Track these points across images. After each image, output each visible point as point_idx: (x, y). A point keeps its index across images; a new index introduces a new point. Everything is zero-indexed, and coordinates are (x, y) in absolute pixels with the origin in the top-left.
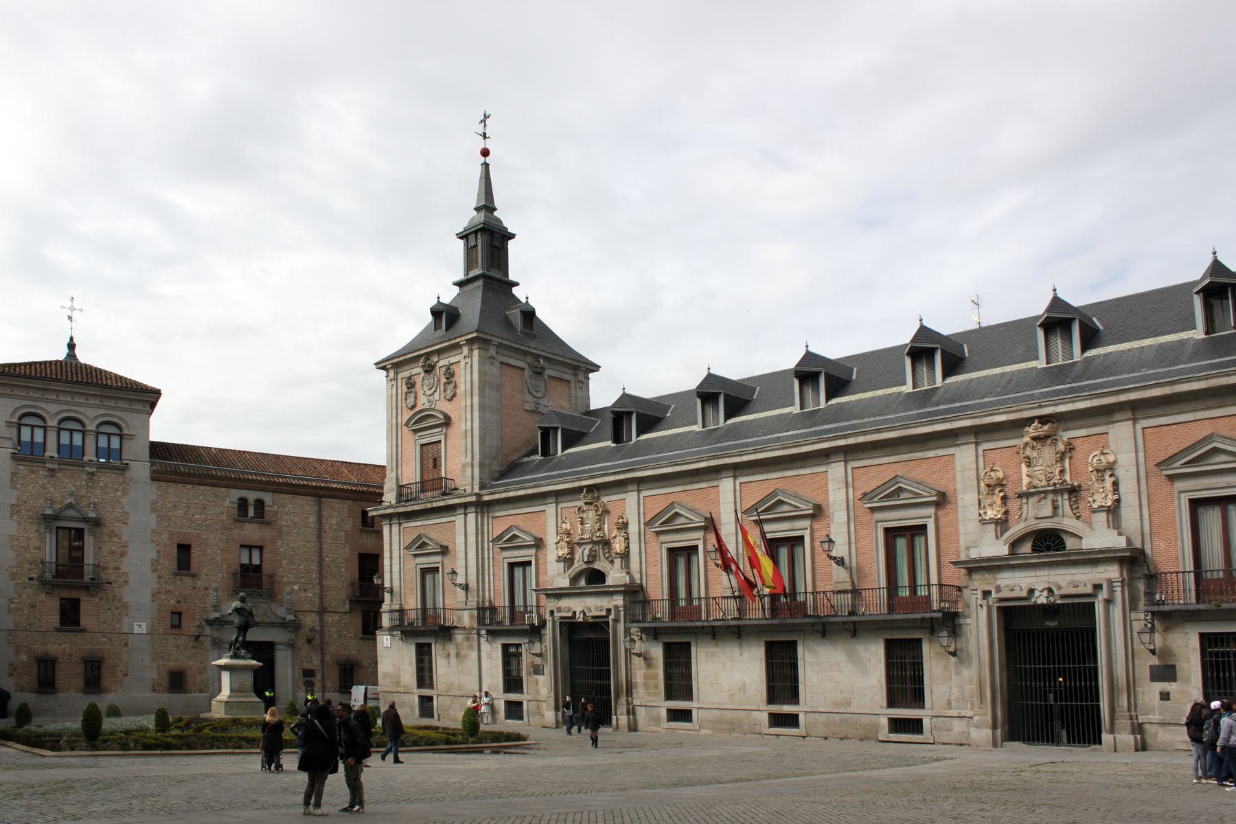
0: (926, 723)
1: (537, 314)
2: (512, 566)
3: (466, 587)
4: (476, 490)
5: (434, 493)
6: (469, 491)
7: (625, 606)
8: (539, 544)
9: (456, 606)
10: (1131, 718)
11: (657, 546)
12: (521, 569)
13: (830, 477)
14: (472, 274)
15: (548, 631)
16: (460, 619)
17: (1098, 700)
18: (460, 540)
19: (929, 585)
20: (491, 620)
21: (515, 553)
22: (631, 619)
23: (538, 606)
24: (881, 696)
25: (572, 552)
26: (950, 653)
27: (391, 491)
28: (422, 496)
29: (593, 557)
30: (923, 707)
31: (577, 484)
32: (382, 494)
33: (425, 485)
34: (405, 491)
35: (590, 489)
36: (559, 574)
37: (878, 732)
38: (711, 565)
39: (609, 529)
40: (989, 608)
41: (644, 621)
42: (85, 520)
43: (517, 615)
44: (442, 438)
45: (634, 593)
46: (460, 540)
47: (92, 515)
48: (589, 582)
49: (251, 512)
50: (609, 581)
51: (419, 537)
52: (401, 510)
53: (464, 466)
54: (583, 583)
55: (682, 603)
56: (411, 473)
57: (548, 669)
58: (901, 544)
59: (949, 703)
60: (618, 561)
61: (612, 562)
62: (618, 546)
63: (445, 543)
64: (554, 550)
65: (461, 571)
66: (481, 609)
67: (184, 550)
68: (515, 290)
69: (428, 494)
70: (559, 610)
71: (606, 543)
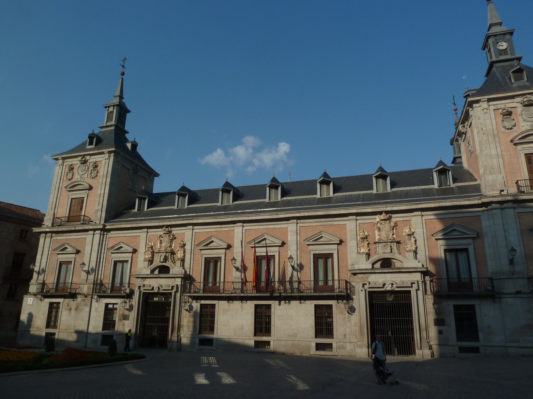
0: (334, 345)
1: (138, 147)
2: (116, 263)
3: (88, 273)
4: (102, 222)
6: (98, 222)
7: (182, 285)
8: (135, 251)
12: (121, 264)
14: (109, 124)
21: (120, 255)
22: (184, 291)
25: (153, 257)
27: (48, 220)
29: (166, 259)
32: (43, 221)
33: (70, 219)
35: (167, 226)
36: (144, 268)
37: (310, 350)
44: (86, 196)
45: (187, 278)
46: (88, 248)
48: (160, 272)
51: (63, 245)
53: (97, 210)
54: (156, 272)
55: (210, 285)
56: (63, 212)
57: (133, 315)
58: (321, 262)
59: (345, 335)
60: (178, 263)
62: (179, 255)
63: (79, 249)
64: (142, 256)
68: (127, 135)
70: (144, 286)
71: (173, 253)
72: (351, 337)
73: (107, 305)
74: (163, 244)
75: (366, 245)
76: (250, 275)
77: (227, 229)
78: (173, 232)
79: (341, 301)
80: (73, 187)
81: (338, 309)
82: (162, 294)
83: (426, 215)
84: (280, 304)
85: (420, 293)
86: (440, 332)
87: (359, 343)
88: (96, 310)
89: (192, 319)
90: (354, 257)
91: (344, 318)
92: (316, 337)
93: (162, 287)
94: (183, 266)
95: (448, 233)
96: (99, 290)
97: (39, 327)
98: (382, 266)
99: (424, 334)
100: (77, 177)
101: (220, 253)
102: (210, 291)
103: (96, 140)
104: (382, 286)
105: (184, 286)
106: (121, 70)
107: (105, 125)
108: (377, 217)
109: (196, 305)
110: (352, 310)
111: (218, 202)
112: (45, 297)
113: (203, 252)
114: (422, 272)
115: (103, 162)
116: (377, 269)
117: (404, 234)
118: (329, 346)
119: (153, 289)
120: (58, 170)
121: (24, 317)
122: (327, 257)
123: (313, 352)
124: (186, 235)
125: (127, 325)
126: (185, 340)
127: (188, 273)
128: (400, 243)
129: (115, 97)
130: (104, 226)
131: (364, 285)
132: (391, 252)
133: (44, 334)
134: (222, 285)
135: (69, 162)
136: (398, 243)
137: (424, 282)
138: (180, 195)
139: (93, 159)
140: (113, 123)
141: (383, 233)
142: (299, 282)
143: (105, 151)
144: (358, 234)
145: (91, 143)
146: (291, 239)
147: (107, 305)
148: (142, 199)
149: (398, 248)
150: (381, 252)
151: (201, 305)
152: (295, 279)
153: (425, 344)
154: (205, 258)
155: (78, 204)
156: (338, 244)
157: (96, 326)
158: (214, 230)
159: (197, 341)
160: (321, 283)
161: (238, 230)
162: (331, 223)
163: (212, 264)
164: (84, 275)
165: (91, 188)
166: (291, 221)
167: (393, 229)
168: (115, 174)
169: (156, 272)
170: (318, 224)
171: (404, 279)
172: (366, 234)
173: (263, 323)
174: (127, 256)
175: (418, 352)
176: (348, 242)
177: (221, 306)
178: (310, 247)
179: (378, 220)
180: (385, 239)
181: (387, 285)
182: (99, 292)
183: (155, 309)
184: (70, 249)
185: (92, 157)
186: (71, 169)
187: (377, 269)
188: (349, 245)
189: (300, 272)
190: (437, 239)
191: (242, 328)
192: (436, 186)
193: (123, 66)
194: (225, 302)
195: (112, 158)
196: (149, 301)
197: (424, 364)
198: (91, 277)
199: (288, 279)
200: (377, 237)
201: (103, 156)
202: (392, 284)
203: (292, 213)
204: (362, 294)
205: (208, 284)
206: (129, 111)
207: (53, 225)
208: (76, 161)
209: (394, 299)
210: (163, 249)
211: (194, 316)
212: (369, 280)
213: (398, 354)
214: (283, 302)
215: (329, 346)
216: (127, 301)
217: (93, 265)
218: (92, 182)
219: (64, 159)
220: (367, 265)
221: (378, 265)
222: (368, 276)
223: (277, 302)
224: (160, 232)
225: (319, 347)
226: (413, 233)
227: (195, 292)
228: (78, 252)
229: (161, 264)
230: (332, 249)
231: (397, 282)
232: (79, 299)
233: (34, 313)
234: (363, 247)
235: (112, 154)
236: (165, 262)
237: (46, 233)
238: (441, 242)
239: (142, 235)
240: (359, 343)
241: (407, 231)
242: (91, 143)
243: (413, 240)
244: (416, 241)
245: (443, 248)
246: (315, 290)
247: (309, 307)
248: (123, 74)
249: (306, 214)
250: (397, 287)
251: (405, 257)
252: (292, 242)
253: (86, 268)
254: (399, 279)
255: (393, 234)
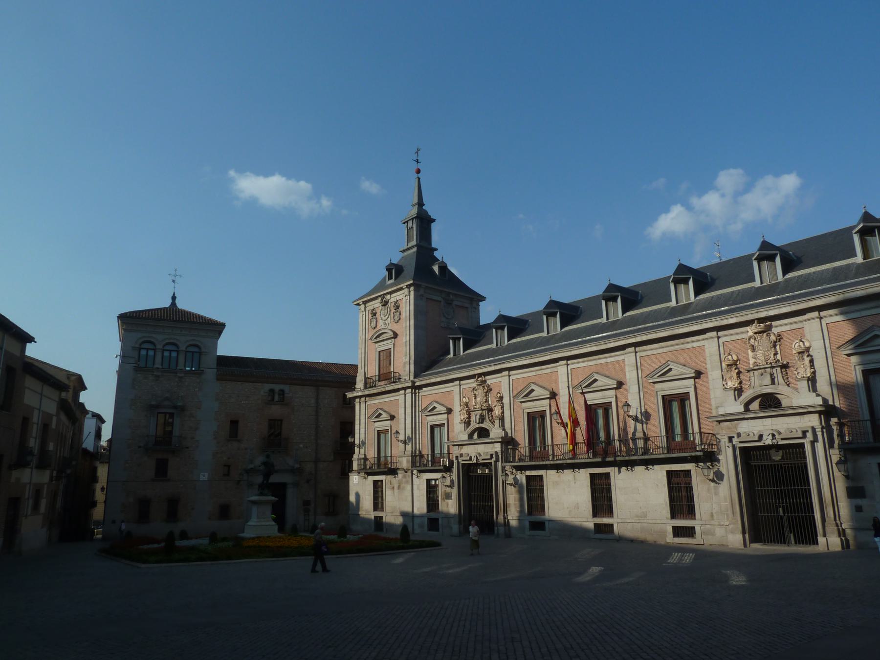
0: (698, 529)
2: (433, 427)
3: (405, 443)
4: (412, 378)
5: (386, 382)
7: (502, 452)
8: (449, 411)
9: (401, 456)
10: (837, 525)
11: (521, 412)
13: (626, 363)
14: (410, 245)
15: (455, 470)
16: (401, 463)
17: (813, 512)
18: (402, 411)
19: (693, 433)
20: (420, 462)
21: (435, 417)
23: (449, 453)
24: (666, 511)
25: (469, 417)
26: (710, 480)
28: (379, 384)
29: (482, 419)
30: (695, 519)
31: (472, 373)
32: (355, 383)
34: (369, 381)
35: (480, 375)
37: (666, 536)
38: (554, 423)
39: (492, 400)
40: (734, 447)
41: (514, 461)
42: (175, 407)
43: (436, 460)
45: (508, 442)
47: (180, 404)
48: (479, 437)
49: (276, 398)
50: (492, 435)
52: (367, 393)
53: (405, 363)
54: (476, 436)
55: (539, 449)
56: (373, 371)
57: (454, 492)
58: (675, 405)
60: (497, 422)
61: (493, 423)
62: (497, 412)
64: (458, 417)
65: (402, 432)
66: (414, 457)
67: (234, 423)
68: (436, 254)
69: (382, 383)
70: (461, 455)
71: (490, 410)
72: (719, 515)
73: (428, 481)
74: (478, 399)
75: (735, 376)
76: (581, 435)
77: (549, 371)
78: (488, 382)
79: (702, 464)
80: (378, 337)
81: (698, 476)
82: (484, 465)
83: (827, 316)
84: (619, 472)
85: (819, 446)
86: (859, 509)
87: (731, 526)
88: (418, 489)
89: (517, 496)
90: (719, 398)
91: (709, 490)
92: (673, 517)
93: (480, 455)
94: (503, 426)
95: (861, 344)
96: (419, 463)
97: (367, 508)
98: (762, 407)
99: (830, 512)
100: (381, 324)
101: (543, 405)
102: (535, 457)
103: (395, 271)
104: (756, 439)
105: (504, 452)
106: (415, 166)
107: (406, 247)
108: (748, 328)
109: (522, 477)
110: (719, 477)
111: (543, 331)
112: (369, 474)
113: (524, 405)
114: (820, 413)
115: (404, 300)
116: (755, 411)
117: (794, 352)
118: (689, 532)
119: (470, 459)
120: (361, 317)
121: (352, 498)
122: (683, 398)
123: (670, 539)
124: (501, 383)
125: (450, 506)
126: (514, 522)
127: (510, 435)
128: (789, 367)
129: (413, 206)
130: (413, 382)
131: (730, 439)
132: (773, 382)
133: (373, 518)
134: (550, 448)
135: (371, 306)
136: (785, 367)
137: (828, 428)
138: (497, 328)
139: (393, 299)
140: (414, 243)
141: (760, 354)
142: (646, 439)
143: (403, 285)
144: (723, 359)
145: (390, 278)
146: (630, 376)
147: (428, 481)
148: (456, 340)
149: (786, 377)
150: (758, 384)
151: (527, 477)
152: (639, 434)
153: (831, 528)
154: (528, 413)
155: (386, 357)
156: (695, 378)
157: (421, 506)
158: (534, 374)
159: (527, 524)
160: (678, 439)
161: (561, 369)
162: (682, 346)
163: (535, 420)
164: (402, 446)
165: (395, 335)
166: (628, 350)
167: (775, 346)
168: (419, 313)
169: (476, 436)
170: (665, 350)
171: (792, 426)
172: (735, 358)
173: (602, 498)
174: (442, 419)
175: (821, 540)
176: (709, 373)
177: (550, 476)
178: (657, 386)
179: (751, 333)
180: (762, 363)
181: (765, 437)
182: (420, 466)
183: (476, 483)
184: (384, 416)
185: (393, 295)
186: (374, 314)
187: (755, 411)
188: (710, 377)
189: (647, 424)
190: (849, 355)
191: (577, 506)
192: (859, 259)
193: (417, 161)
194: (553, 472)
195: (412, 293)
196: (471, 474)
197: (829, 556)
198: (409, 447)
199: (630, 436)
200: (752, 361)
201: (402, 292)
202: (773, 435)
203: (624, 339)
204: (730, 451)
205: (535, 449)
206: (434, 220)
207: (365, 387)
208: (377, 304)
209: (783, 457)
210: (478, 406)
211: (520, 492)
212: (739, 431)
213: (796, 543)
214: (623, 469)
215: (689, 532)
216: (447, 475)
217: (409, 432)
218: (396, 328)
219: (365, 303)
220: (737, 407)
221: (755, 406)
222: (737, 424)
223: (617, 469)
224: (473, 383)
225: (678, 531)
226: (808, 349)
227: (520, 460)
228: (392, 418)
229: (478, 426)
230: (686, 386)
231: (782, 431)
232: (400, 474)
233: (361, 494)
234: (730, 378)
235: (412, 288)
236: (482, 423)
237: (360, 397)
238: (854, 359)
239: (454, 388)
240: (731, 526)
241: (797, 346)
242: (390, 278)
243: (807, 360)
244: (812, 361)
245: (859, 369)
246: (669, 449)
247: (659, 473)
248: (418, 171)
249: (644, 338)
250: (782, 439)
251: (796, 390)
252: (631, 378)
253: (402, 437)
254: (785, 426)
255: (776, 354)
